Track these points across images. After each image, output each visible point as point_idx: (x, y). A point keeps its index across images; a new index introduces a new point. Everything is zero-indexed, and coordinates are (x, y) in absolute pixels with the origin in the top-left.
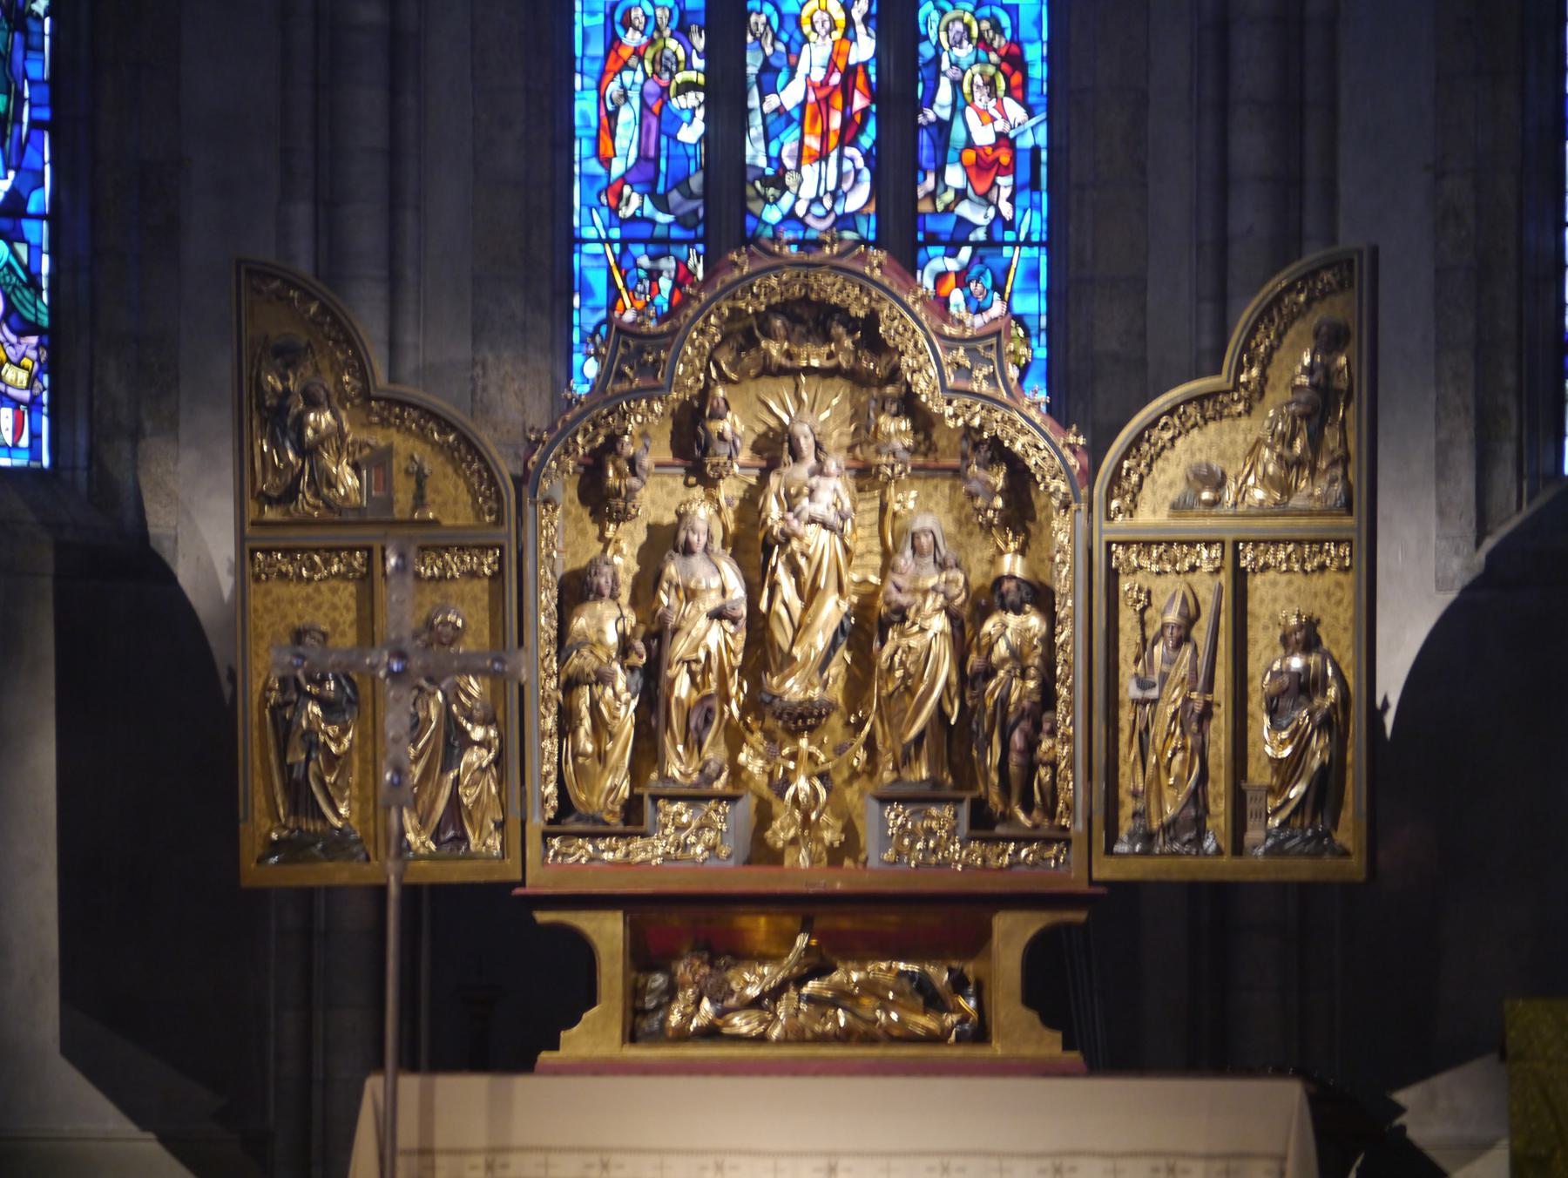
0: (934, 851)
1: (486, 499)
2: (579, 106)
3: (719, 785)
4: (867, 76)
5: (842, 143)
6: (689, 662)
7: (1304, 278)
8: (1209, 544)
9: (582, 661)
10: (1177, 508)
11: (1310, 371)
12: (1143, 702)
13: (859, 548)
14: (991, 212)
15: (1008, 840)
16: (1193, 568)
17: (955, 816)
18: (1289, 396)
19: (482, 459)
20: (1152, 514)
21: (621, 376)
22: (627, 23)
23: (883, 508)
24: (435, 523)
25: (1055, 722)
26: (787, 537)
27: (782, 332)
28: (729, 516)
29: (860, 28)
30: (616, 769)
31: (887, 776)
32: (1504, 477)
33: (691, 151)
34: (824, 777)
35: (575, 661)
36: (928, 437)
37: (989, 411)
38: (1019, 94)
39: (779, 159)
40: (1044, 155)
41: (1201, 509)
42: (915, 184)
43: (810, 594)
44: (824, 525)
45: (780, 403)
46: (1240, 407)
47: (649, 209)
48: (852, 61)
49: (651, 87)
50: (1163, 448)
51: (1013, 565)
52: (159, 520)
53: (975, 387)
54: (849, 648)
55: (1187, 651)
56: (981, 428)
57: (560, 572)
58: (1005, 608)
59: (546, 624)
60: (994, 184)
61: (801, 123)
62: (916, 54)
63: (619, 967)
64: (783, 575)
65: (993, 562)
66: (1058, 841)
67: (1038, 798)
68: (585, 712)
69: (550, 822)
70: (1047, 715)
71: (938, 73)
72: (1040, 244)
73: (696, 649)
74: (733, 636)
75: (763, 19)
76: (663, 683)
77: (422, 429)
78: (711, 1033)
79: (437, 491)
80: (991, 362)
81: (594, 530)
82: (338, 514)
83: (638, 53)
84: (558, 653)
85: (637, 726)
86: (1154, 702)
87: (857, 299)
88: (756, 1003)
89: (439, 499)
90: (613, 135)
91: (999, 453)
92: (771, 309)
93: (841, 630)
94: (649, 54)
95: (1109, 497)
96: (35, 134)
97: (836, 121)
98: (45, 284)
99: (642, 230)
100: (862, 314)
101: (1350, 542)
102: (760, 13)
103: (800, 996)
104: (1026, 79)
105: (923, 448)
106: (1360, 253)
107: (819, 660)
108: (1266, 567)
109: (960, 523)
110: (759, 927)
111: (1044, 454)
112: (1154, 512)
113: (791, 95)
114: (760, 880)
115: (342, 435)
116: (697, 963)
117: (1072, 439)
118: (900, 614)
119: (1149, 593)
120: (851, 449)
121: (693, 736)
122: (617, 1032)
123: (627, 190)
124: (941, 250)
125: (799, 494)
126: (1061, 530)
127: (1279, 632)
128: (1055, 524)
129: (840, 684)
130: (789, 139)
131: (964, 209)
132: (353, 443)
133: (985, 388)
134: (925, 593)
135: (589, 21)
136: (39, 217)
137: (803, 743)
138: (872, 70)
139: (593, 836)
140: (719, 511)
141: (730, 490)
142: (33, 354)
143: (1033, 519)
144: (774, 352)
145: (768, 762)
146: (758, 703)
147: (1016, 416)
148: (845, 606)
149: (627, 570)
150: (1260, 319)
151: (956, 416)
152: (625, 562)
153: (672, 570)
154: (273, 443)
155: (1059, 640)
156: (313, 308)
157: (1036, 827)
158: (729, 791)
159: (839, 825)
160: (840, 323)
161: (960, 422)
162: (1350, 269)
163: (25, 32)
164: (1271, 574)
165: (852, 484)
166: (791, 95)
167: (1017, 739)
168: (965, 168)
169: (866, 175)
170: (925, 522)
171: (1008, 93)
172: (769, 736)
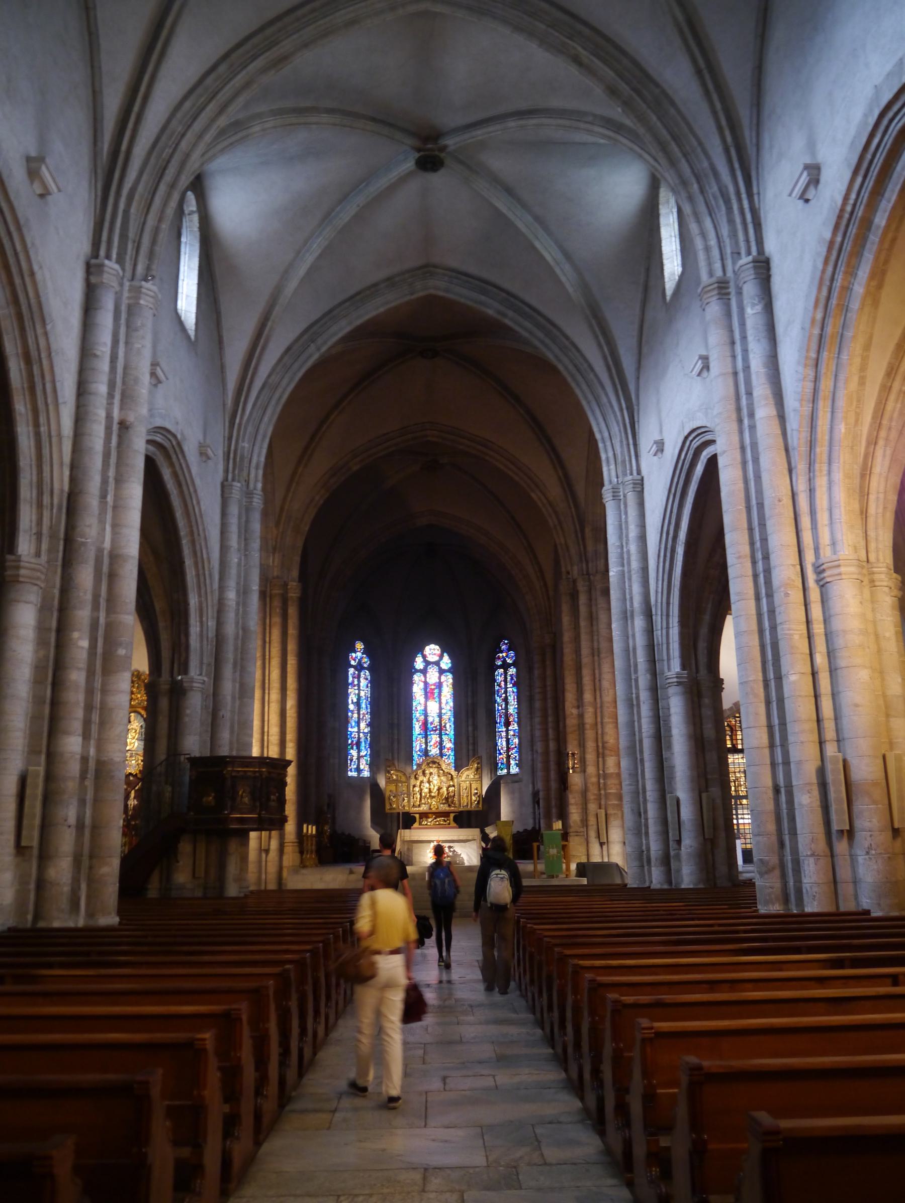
9: (415, 792)
20: (463, 779)
32: (493, 775)
45: (431, 770)
51: (451, 783)
52: (379, 781)
59: (411, 789)
82: (394, 780)
91: (450, 774)
110: (430, 815)
114: (430, 811)
118: (442, 788)
126: (455, 780)
130: (432, 747)
141: (427, 777)
146: (430, 796)
152: (418, 784)
166: (432, 743)
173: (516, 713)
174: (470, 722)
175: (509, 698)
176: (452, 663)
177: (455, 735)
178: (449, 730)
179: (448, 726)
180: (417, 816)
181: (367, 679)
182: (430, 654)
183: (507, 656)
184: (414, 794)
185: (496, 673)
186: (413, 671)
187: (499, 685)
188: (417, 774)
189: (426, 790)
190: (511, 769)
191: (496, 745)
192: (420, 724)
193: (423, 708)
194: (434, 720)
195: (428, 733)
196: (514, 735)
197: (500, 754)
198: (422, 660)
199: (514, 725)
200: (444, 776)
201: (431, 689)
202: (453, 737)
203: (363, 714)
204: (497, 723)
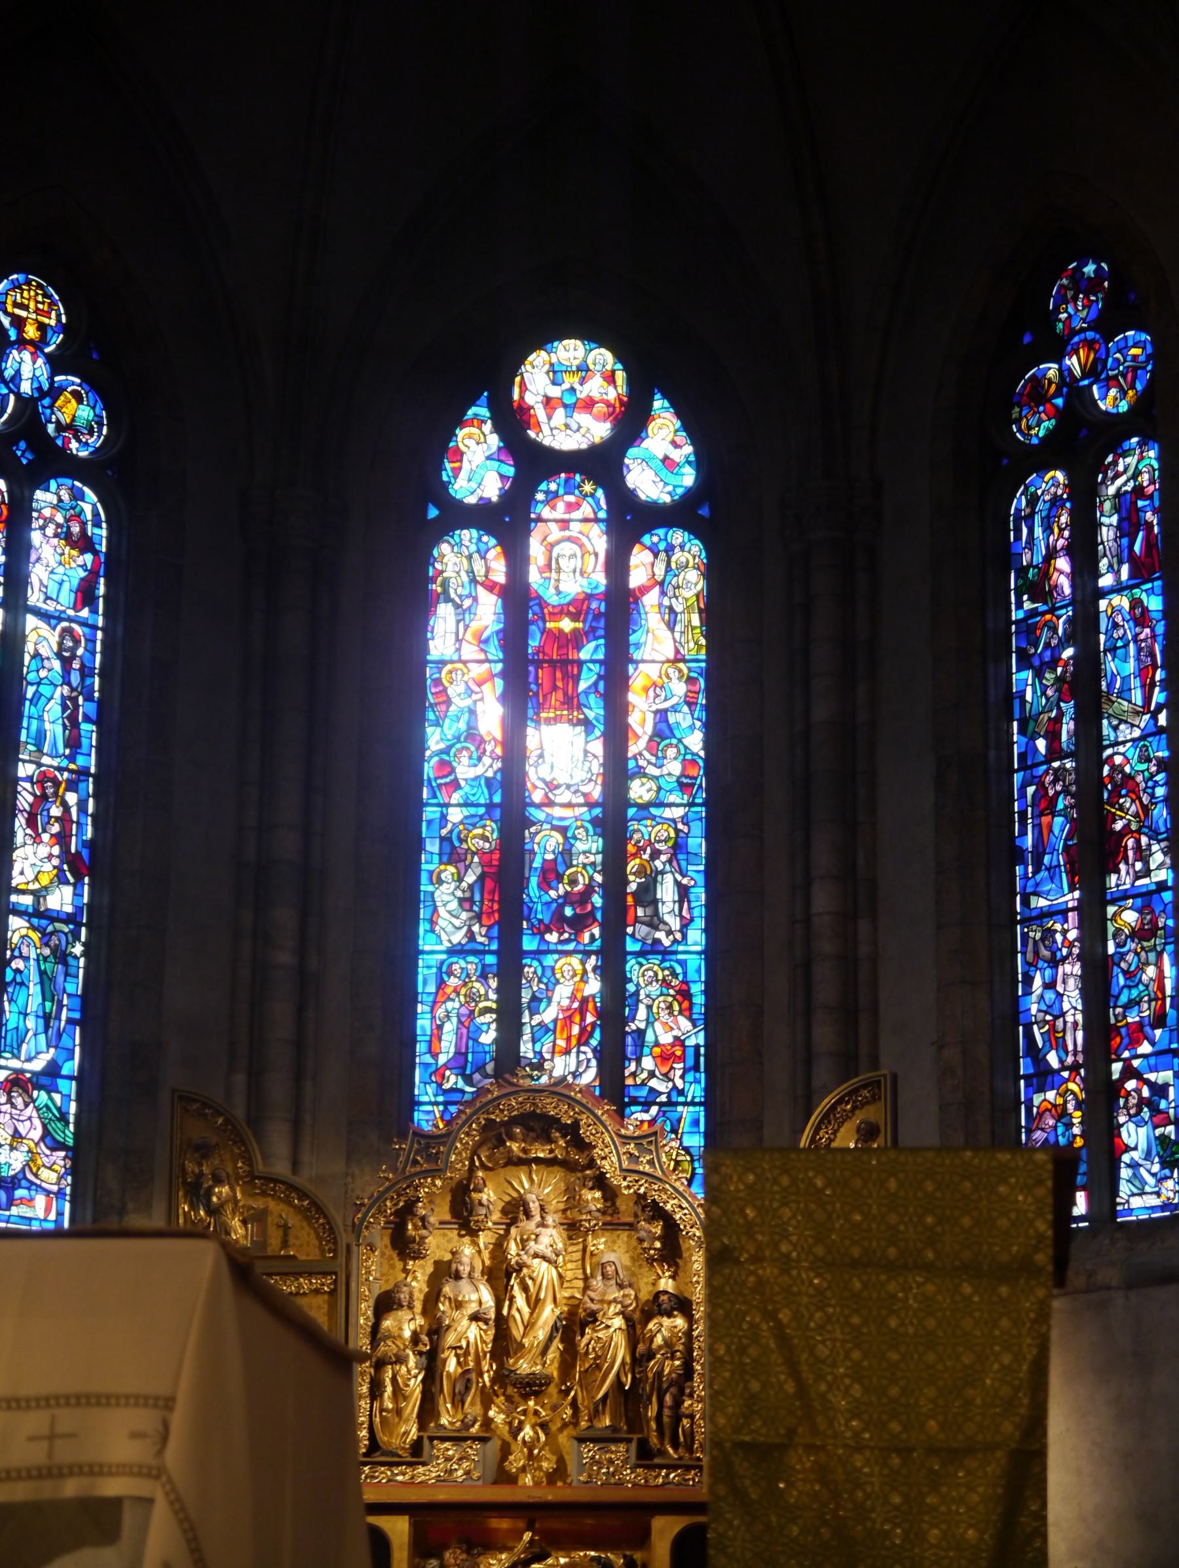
0: (613, 1475)
1: (328, 1242)
2: (419, 1023)
3: (474, 1430)
4: (595, 1003)
5: (579, 1044)
6: (455, 1348)
7: (849, 1094)
9: (387, 1348)
13: (569, 1275)
14: (670, 1085)
15: (661, 1467)
17: (627, 1451)
19: (325, 1217)
21: (415, 1162)
22: (450, 973)
23: (584, 1250)
24: (294, 1257)
25: (692, 1388)
26: (521, 1266)
27: (520, 1136)
28: (486, 1255)
29: (591, 975)
30: (408, 1420)
31: (583, 1424)
33: (487, 1049)
34: (544, 1426)
35: (382, 1348)
36: (614, 1204)
37: (650, 1184)
38: (687, 1013)
39: (540, 1053)
40: (702, 1050)
42: (624, 1068)
43: (535, 1304)
44: (544, 1258)
45: (522, 1182)
47: (461, 1084)
48: (586, 994)
49: (464, 1011)
51: (666, 1284)
53: (641, 1168)
54: (562, 1341)
56: (645, 1195)
57: (377, 1292)
58: (662, 1315)
60: (672, 1068)
61: (554, 1032)
62: (625, 990)
63: (405, 1554)
64: (517, 1291)
65: (654, 1284)
66: (694, 1467)
67: (682, 1439)
68: (388, 1382)
70: (688, 1384)
71: (638, 1001)
72: (700, 1104)
73: (460, 1341)
74: (485, 1331)
75: (532, 970)
76: (439, 1364)
77: (287, 1197)
79: (297, 1238)
80: (651, 1152)
81: (399, 1265)
83: (456, 991)
84: (372, 1343)
85: (423, 1392)
87: (566, 1112)
89: (298, 1243)
90: (440, 1040)
91: (657, 1212)
92: (514, 1121)
93: (555, 1328)
94: (463, 991)
96: (70, 1027)
97: (576, 1030)
98: (72, 1119)
99: (456, 1097)
102: (530, 966)
104: (691, 1005)
105: (610, 1211)
106: (885, 1076)
107: (541, 1346)
109: (633, 1259)
113: (549, 1014)
114: (502, 1494)
115: (236, 1202)
116: (458, 1551)
118: (592, 1318)
120: (564, 1211)
121: (458, 1398)
123: (448, 1073)
124: (639, 1108)
125: (528, 1239)
129: (556, 1364)
130: (548, 1040)
131: (653, 1083)
132: (243, 1207)
133: (647, 1169)
134: (610, 1303)
135: (426, 971)
136: (70, 1078)
137: (531, 1403)
138: (598, 1000)
139: (391, 1465)
140: (479, 1252)
141: (485, 1239)
142: (62, 1163)
143: (681, 1257)
145: (508, 1416)
146: (503, 1377)
147: (667, 1186)
148: (557, 1312)
149: (420, 1291)
150: (821, 1122)
151: (628, 1187)
152: (418, 1285)
153: (447, 1289)
154: (192, 1207)
155: (695, 1333)
156: (220, 1121)
157: (680, 1458)
158: (481, 1434)
159: (554, 1458)
160: (558, 1130)
161: (632, 1191)
163: (66, 964)
165: (565, 1234)
166: (549, 1014)
167: (668, 1399)
168: (654, 1058)
169: (594, 1063)
170: (610, 1257)
171: (681, 1012)
172: (509, 1399)
173: (1162, 765)
174: (823, 857)
175: (1111, 665)
176: (702, 462)
177: (710, 954)
178: (675, 923)
179: (667, 891)
180: (398, 1528)
181: (84, 544)
182: (548, 402)
183: (1093, 372)
184: (380, 1365)
185: (1020, 502)
186: (433, 513)
187: (1040, 588)
188: (407, 1211)
189: (469, 1334)
190: (1124, 1189)
191: (1014, 1013)
192: (470, 878)
193: (489, 767)
194: (567, 853)
195: (529, 943)
196: (1140, 934)
197: (1043, 1077)
198: (494, 441)
199: (1143, 855)
200: (612, 1226)
201: (558, 637)
202: (695, 965)
203: (43, 779)
204: (1018, 856)
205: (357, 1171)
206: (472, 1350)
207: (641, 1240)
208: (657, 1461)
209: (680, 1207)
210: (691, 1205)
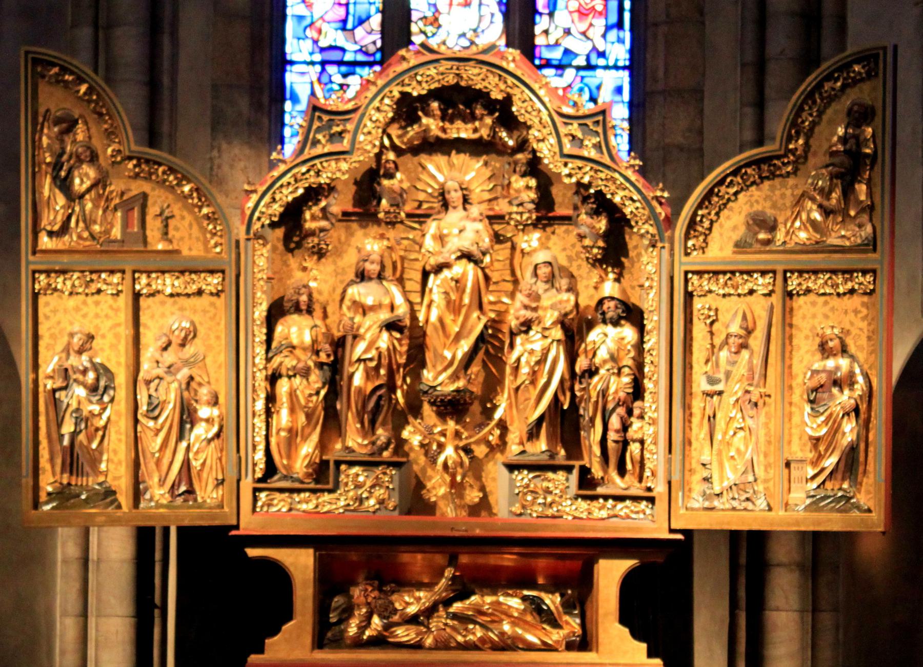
0: (551, 505)
7: (840, 69)
8: (763, 273)
10: (740, 246)
11: (844, 140)
12: (710, 395)
13: (495, 276)
16: (751, 292)
18: (827, 160)
25: (643, 409)
27: (438, 113)
31: (514, 448)
41: (758, 246)
42: (533, 23)
46: (789, 169)
50: (729, 200)
53: (585, 153)
55: (745, 354)
56: (590, 185)
58: (604, 322)
63: (310, 591)
65: (596, 288)
69: (260, 480)
70: (637, 404)
72: (624, 68)
74: (399, 340)
78: (379, 642)
80: (597, 133)
86: (720, 393)
88: (413, 620)
92: (434, 94)
95: (687, 237)
99: (335, 56)
100: (500, 97)
101: (874, 272)
103: (448, 613)
106: (885, 49)
108: (808, 291)
110: (416, 561)
111: (638, 204)
112: (721, 249)
116: (370, 589)
117: (659, 193)
119: (717, 310)
122: (308, 640)
127: (818, 340)
128: (645, 259)
133: (593, 154)
139: (291, 491)
143: (626, 255)
144: (433, 127)
147: (617, 175)
150: (804, 102)
151: (570, 175)
155: (647, 346)
156: (83, 88)
161: (574, 180)
162: (877, 64)
164: (812, 297)
167: (615, 422)
205: (224, 146)
206: (385, 361)
207: (581, 237)
208: (600, 490)
209: (632, 199)
210: (644, 198)
